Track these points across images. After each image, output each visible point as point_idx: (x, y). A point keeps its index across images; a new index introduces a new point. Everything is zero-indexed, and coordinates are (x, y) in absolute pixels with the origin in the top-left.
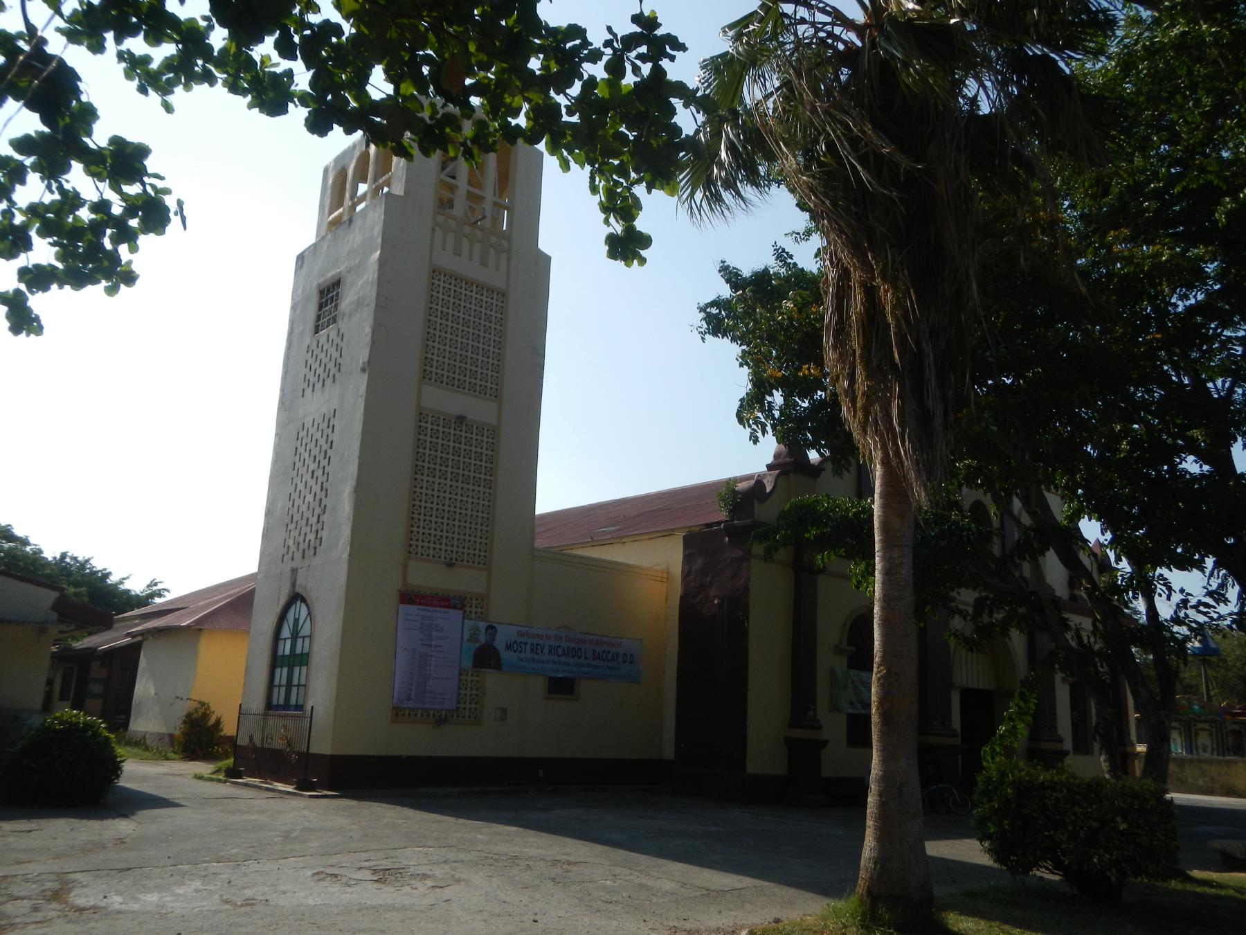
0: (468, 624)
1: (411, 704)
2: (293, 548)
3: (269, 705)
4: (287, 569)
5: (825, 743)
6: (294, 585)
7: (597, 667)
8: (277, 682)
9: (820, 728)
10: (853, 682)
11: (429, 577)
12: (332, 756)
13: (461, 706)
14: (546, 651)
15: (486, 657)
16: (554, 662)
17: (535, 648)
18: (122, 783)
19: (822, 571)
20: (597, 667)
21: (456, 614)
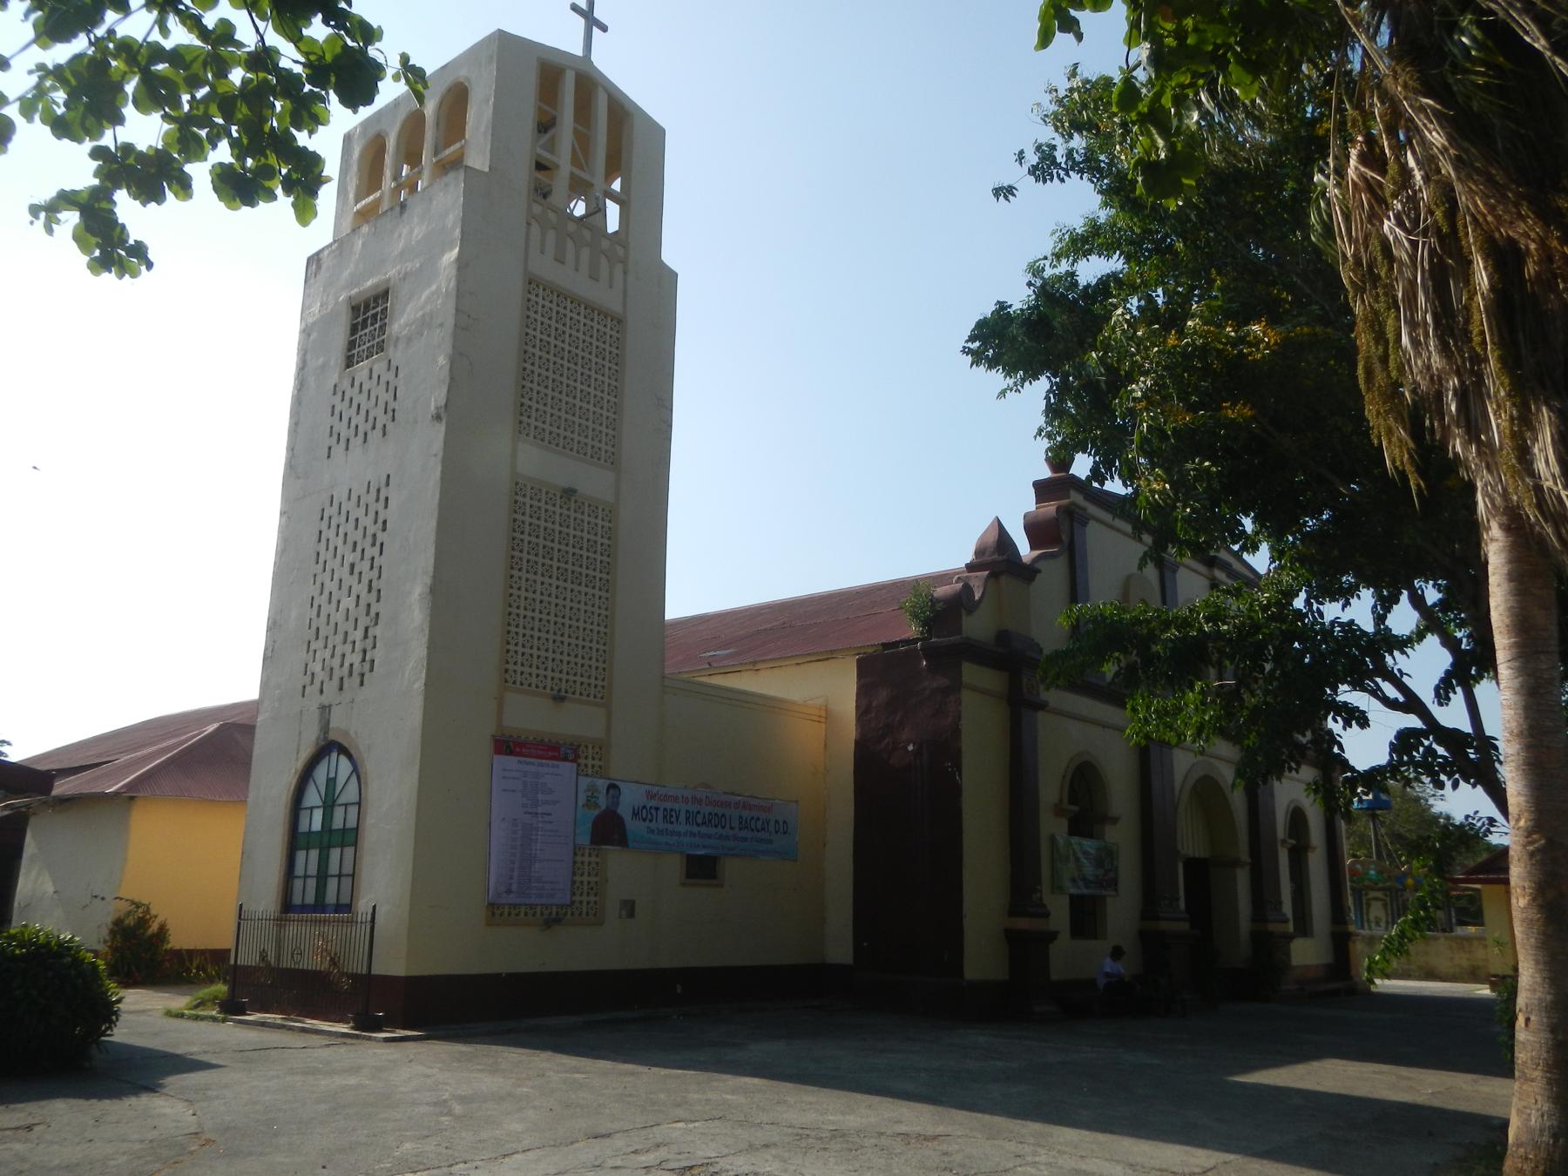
0: (584, 782)
1: (512, 899)
2: (321, 675)
3: (287, 906)
4: (313, 703)
5: (1053, 936)
6: (325, 727)
7: (745, 840)
8: (299, 870)
9: (1047, 915)
10: (1075, 853)
11: (530, 716)
12: (407, 978)
13: (577, 898)
15: (609, 830)
16: (693, 834)
17: (669, 816)
18: (120, 1034)
19: (1042, 706)
20: (745, 840)
21: (567, 768)
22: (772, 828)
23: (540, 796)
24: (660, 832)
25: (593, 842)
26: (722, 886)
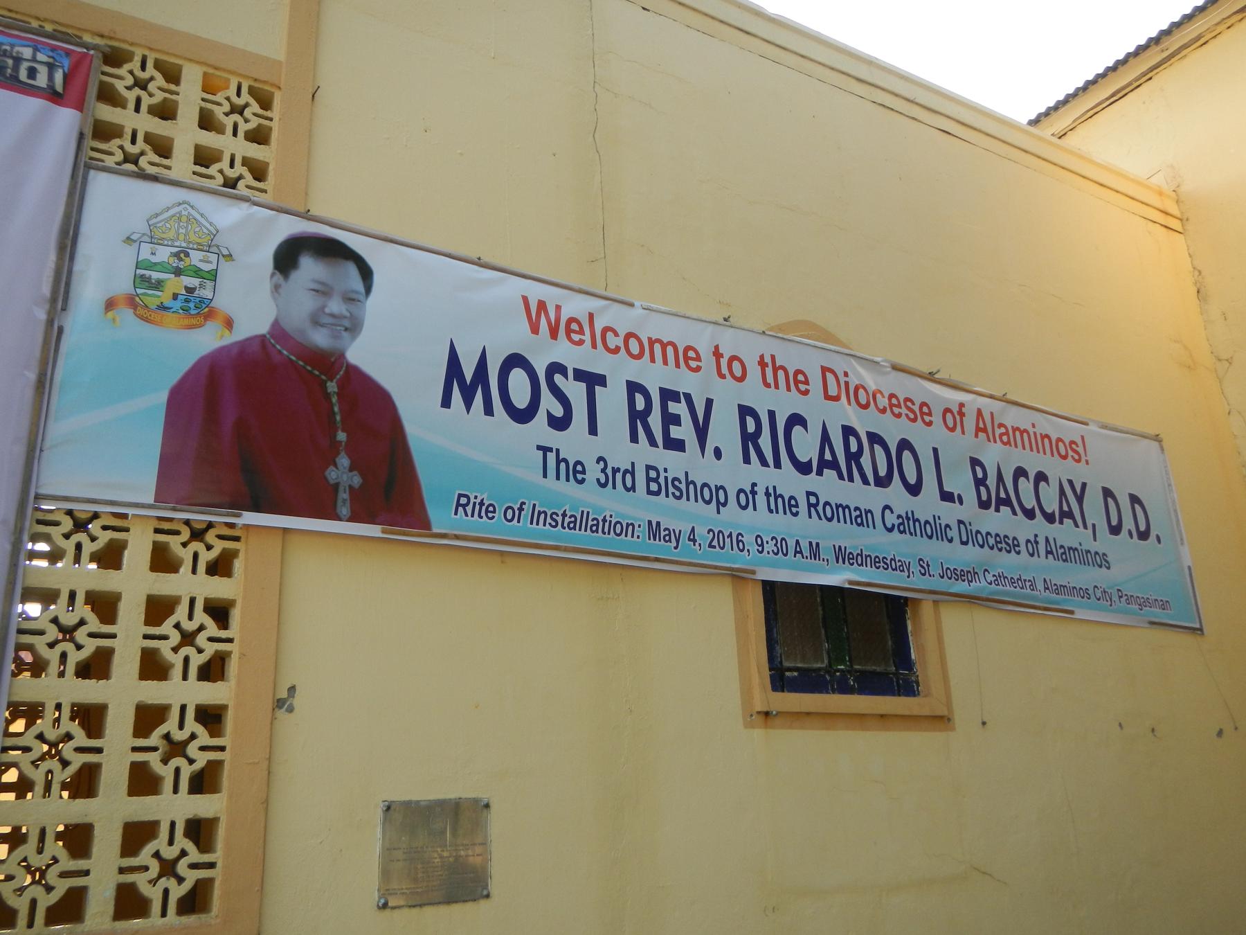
0: (117, 204)
7: (1008, 544)
14: (725, 430)
20: (1008, 544)
24: (611, 477)
25: (173, 479)
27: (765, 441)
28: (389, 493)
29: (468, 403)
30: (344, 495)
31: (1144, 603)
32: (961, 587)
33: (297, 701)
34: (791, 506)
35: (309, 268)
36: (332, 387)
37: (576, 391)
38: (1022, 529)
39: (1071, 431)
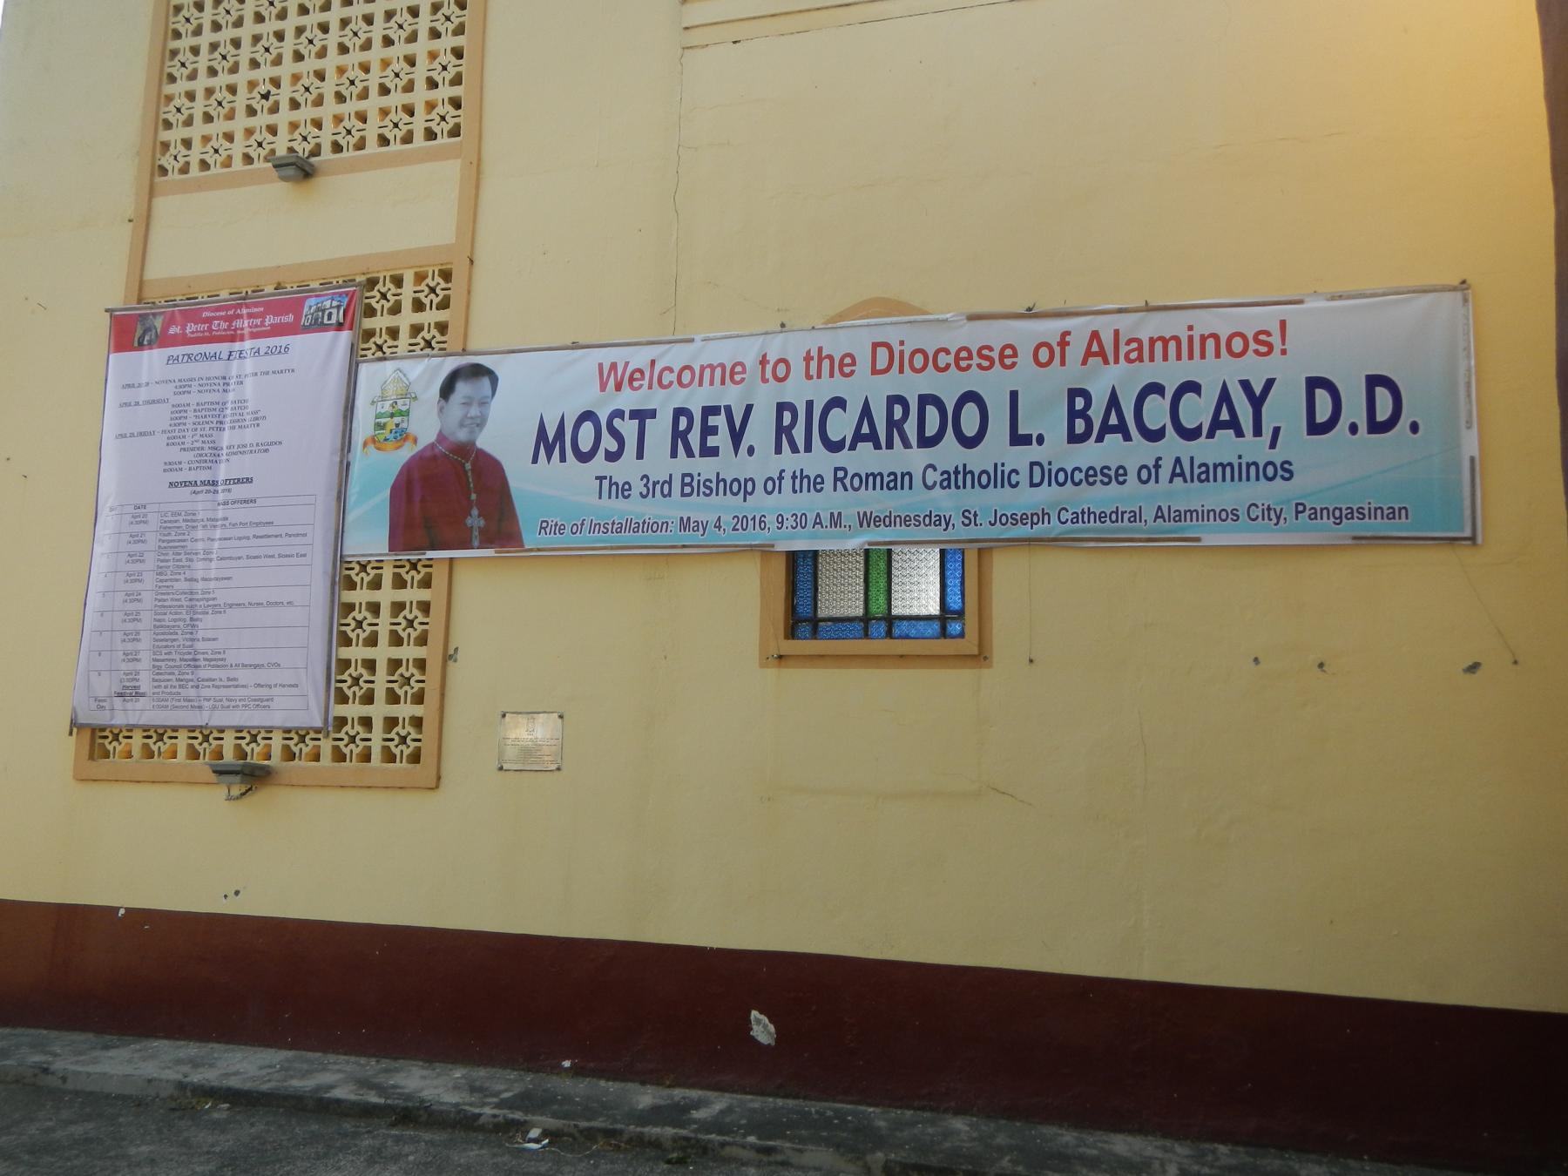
7: (1120, 475)
14: (760, 431)
15: (451, 500)
16: (807, 482)
17: (694, 432)
22: (1285, 408)
23: (227, 438)
24: (652, 488)
26: (980, 657)
27: (799, 433)
28: (501, 529)
29: (549, 458)
30: (476, 533)
31: (1339, 516)
32: (1023, 531)
33: (459, 656)
34: (817, 483)
35: (462, 388)
36: (468, 466)
37: (629, 428)
38: (1138, 452)
39: (1252, 320)
